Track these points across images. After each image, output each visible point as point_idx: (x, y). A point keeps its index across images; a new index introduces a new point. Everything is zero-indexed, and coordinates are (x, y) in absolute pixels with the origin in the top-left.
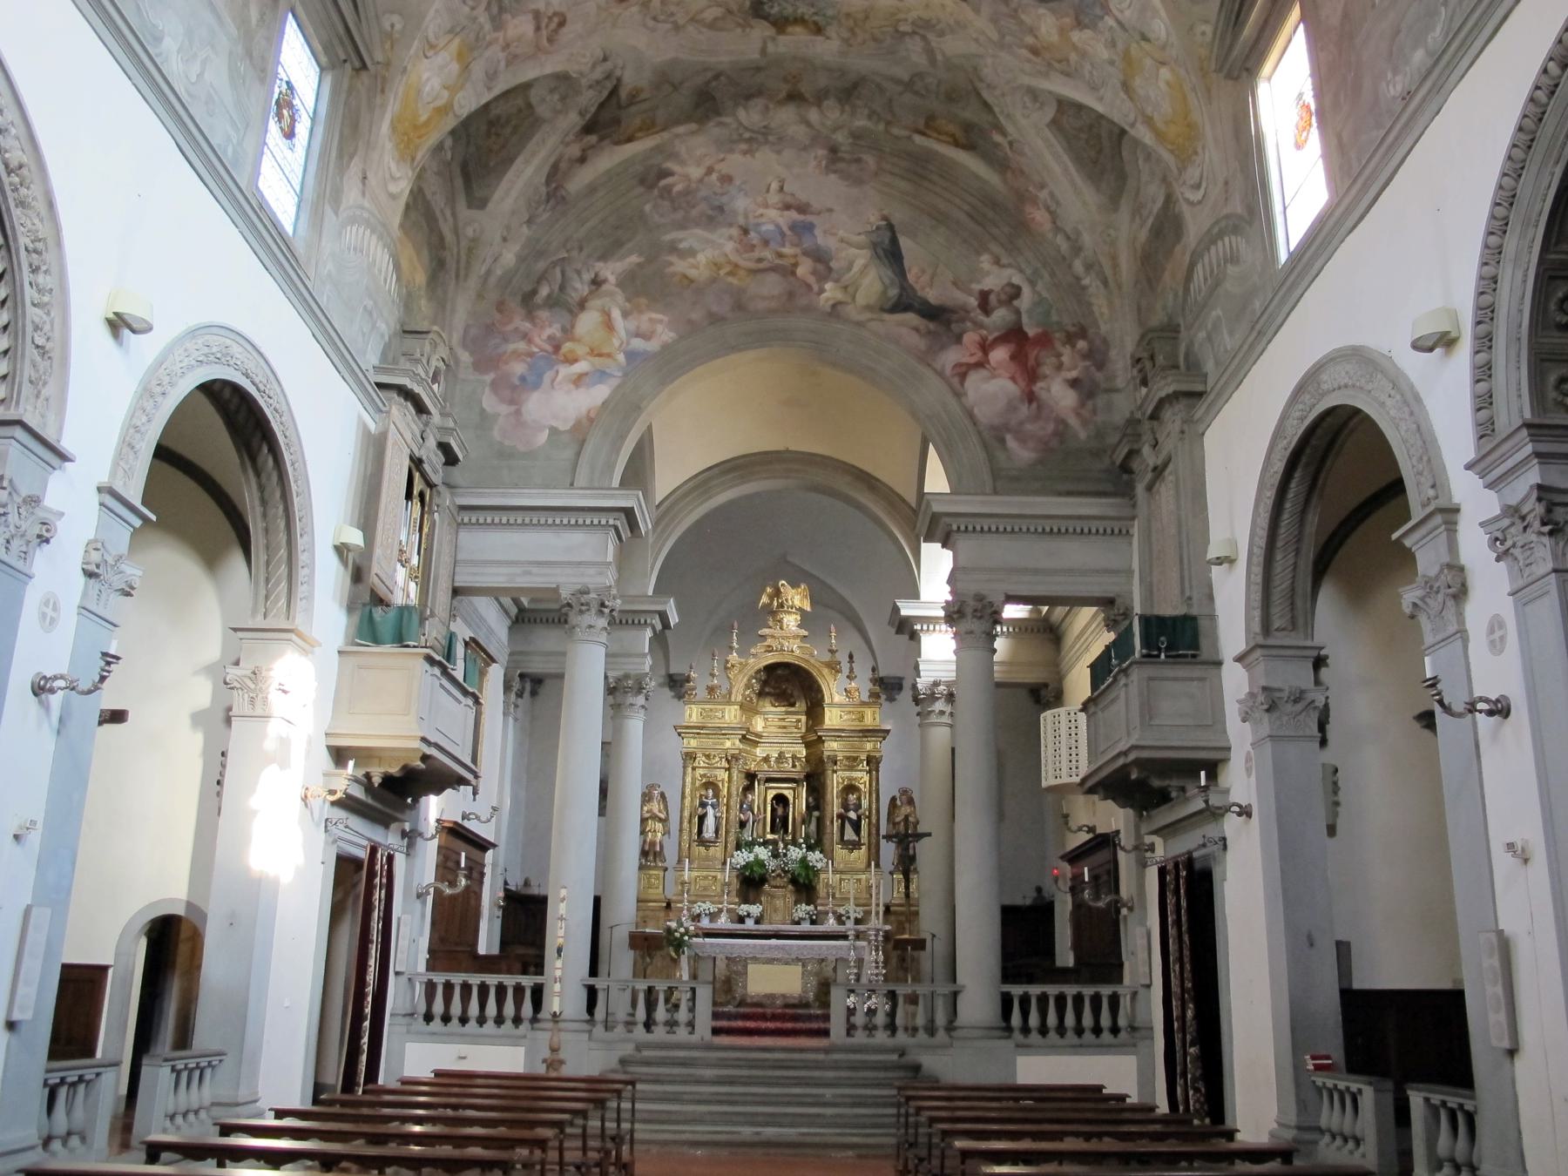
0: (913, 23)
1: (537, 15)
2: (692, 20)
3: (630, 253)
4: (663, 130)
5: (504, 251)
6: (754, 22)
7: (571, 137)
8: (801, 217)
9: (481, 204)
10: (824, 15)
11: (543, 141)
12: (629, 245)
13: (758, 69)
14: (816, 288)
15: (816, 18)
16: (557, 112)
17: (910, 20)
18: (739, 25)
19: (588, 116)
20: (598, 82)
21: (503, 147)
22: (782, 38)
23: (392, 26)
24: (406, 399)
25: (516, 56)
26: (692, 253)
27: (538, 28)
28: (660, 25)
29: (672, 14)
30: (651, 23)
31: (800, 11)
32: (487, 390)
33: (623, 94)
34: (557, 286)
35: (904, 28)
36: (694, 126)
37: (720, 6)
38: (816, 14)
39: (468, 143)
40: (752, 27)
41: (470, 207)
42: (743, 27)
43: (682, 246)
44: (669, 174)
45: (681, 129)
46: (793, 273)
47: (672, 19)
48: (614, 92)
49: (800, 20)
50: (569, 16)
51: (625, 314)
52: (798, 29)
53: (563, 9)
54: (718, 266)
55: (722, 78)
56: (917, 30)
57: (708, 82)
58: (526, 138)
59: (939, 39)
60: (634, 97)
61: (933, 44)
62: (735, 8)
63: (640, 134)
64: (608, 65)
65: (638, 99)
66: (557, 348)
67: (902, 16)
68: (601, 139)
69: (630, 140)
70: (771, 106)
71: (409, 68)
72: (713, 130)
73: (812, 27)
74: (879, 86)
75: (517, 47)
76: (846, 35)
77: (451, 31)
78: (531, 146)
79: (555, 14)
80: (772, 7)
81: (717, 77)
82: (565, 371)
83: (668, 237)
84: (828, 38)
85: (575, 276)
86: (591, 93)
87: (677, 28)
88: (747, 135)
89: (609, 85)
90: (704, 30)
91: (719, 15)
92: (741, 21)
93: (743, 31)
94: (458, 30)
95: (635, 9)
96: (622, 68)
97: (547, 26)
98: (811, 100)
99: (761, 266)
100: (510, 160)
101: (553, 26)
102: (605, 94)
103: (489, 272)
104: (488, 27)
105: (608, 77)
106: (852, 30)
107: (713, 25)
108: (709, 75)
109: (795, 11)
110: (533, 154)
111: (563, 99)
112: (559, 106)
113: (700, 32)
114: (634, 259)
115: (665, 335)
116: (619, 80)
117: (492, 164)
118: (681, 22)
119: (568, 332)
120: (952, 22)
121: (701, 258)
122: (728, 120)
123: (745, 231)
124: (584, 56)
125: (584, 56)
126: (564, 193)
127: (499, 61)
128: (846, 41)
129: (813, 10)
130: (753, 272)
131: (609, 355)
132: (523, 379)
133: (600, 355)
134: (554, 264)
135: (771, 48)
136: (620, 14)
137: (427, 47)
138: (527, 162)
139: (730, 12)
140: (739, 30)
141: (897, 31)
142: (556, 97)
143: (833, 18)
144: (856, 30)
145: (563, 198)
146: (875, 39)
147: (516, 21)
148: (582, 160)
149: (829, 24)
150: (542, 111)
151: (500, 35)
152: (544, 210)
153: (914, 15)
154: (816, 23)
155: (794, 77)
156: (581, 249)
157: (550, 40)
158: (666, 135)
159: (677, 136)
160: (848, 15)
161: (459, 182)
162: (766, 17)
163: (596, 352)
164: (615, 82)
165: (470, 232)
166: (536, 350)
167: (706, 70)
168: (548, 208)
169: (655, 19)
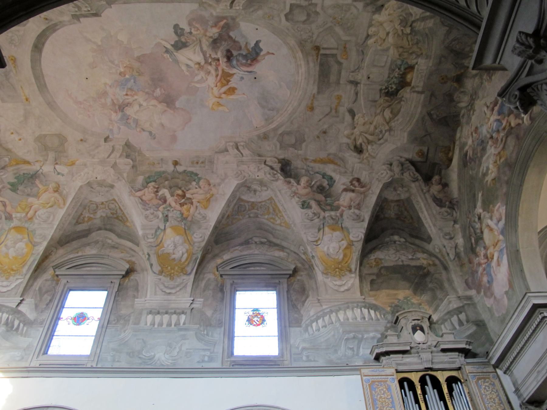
0: (405, 27)
1: (345, 190)
2: (388, 123)
3: (478, 194)
4: (454, 143)
5: (457, 241)
6: (399, 96)
7: (425, 189)
8: (498, 105)
9: (429, 240)
10: (401, 65)
11: (418, 201)
12: (476, 193)
13: (432, 95)
14: (521, 122)
15: (402, 69)
16: (408, 191)
17: (402, 28)
18: (399, 102)
19: (420, 178)
20: (402, 170)
21: (412, 218)
22: (413, 84)
23: (303, 250)
24: (389, 355)
25: (359, 204)
26: (488, 169)
27: (353, 191)
28: (385, 138)
29: (381, 132)
30: (382, 141)
31: (396, 75)
32: (485, 298)
33: (417, 159)
34: (474, 235)
35: (408, 30)
36: (459, 128)
37: (384, 110)
38: (399, 69)
39: (403, 230)
40: (403, 97)
41: (429, 243)
42: (401, 100)
43: (484, 171)
44: (467, 152)
45: (458, 135)
46: (512, 128)
47: (384, 132)
48: (412, 163)
49: (403, 76)
50: (356, 176)
51: (491, 218)
52: (409, 77)
53: (351, 178)
54: (495, 162)
55: (432, 112)
56: (409, 24)
57: (432, 119)
58: (413, 207)
59: (414, 15)
60: (421, 153)
61: (418, 17)
62: (388, 104)
63: (450, 154)
64: (395, 164)
65: (426, 153)
66: (487, 258)
67: (400, 33)
68: (440, 174)
69: (450, 160)
70: (462, 90)
71: (314, 255)
72: (463, 121)
73: (407, 71)
74: (454, 40)
75: (354, 203)
76: (414, 56)
77: (319, 230)
78: (417, 207)
79: (351, 182)
80: (392, 88)
81: (430, 114)
82: (494, 263)
83: (480, 174)
84: (417, 63)
85: (475, 224)
86: (406, 175)
87: (390, 130)
88: (470, 107)
89: (408, 164)
90: (396, 118)
91: (390, 111)
92: (396, 102)
93: (404, 101)
94: (322, 226)
95: (369, 147)
96: (401, 157)
97: (355, 187)
98: (462, 71)
99: (504, 141)
100: (419, 218)
101: (357, 184)
102: (412, 167)
103: (457, 255)
104: (333, 213)
105: (402, 164)
106: (411, 54)
107: (395, 114)
108: (427, 118)
109: (396, 78)
110: (421, 209)
111: (403, 186)
112: (405, 189)
113: (397, 120)
114: (480, 195)
115: (503, 210)
116: (407, 160)
117: (417, 226)
118: (387, 128)
119: (486, 248)
120: (400, 10)
121: (491, 166)
122: (463, 112)
123: (492, 137)
124: (382, 174)
125: (382, 174)
126: (455, 200)
127: (354, 213)
128: (418, 56)
129: (397, 70)
130: (504, 148)
131: (498, 241)
132: (489, 282)
133: (496, 244)
134: (469, 227)
135: (420, 89)
136: (369, 154)
137: (315, 243)
138: (422, 212)
139: (390, 106)
140: (402, 103)
141: (410, 34)
142: (400, 189)
143: (403, 61)
144: (410, 52)
145: (457, 202)
146: (417, 43)
147: (341, 200)
148: (445, 185)
149: (407, 63)
150: (403, 197)
151: (342, 208)
152: (456, 212)
153: (398, 27)
154: (405, 69)
155: (443, 79)
156: (470, 212)
157: (362, 187)
158: (457, 143)
159: (460, 138)
160: (400, 55)
161: (417, 242)
162: (397, 91)
163: (495, 245)
164: (408, 162)
165: (437, 250)
166: (484, 266)
167: (423, 119)
168: (456, 209)
169: (380, 139)
